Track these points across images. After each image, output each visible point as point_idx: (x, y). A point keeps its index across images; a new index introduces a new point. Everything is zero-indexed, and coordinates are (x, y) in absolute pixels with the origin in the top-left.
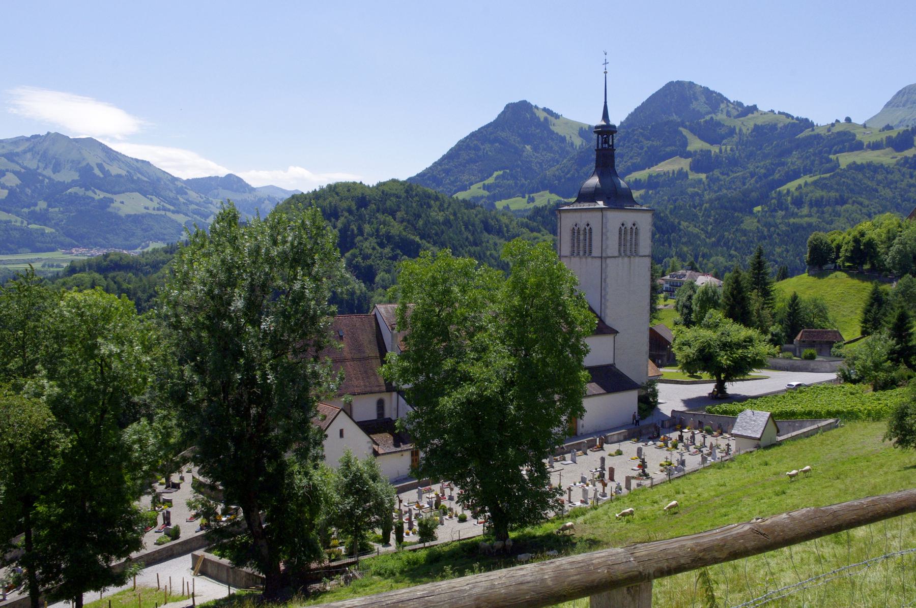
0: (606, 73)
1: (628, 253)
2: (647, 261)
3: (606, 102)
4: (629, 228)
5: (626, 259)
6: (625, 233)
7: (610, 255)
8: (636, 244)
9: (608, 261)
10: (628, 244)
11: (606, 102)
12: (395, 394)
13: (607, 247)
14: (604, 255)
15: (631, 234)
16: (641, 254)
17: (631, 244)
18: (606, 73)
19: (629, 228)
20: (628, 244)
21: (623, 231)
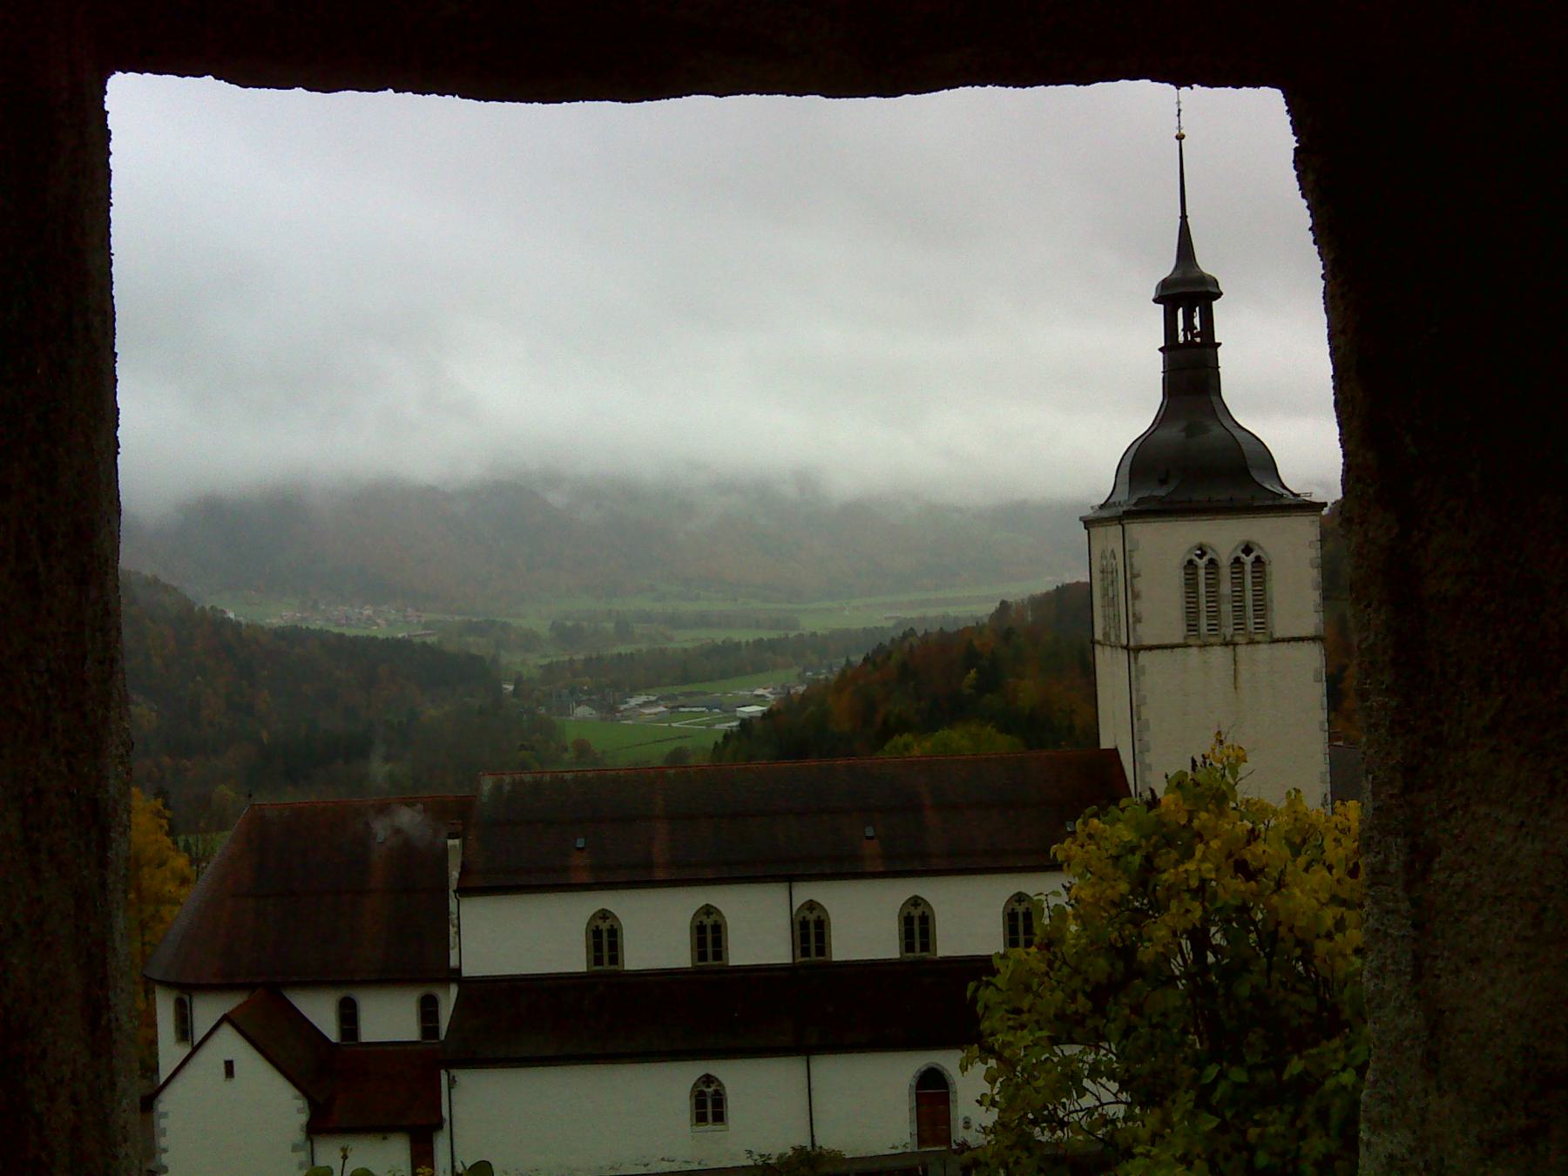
0: (1180, 138)
1: (1228, 631)
2: (1311, 659)
3: (1184, 217)
4: (1225, 560)
5: (1219, 655)
6: (1213, 585)
7: (1147, 642)
8: (1262, 607)
9: (1144, 657)
10: (1226, 608)
11: (1184, 217)
12: (454, 990)
13: (1138, 620)
14: (1132, 644)
15: (1238, 581)
16: (1277, 635)
17: (1239, 609)
18: (1180, 138)
19: (1225, 560)
20: (1226, 608)
21: (1198, 571)
